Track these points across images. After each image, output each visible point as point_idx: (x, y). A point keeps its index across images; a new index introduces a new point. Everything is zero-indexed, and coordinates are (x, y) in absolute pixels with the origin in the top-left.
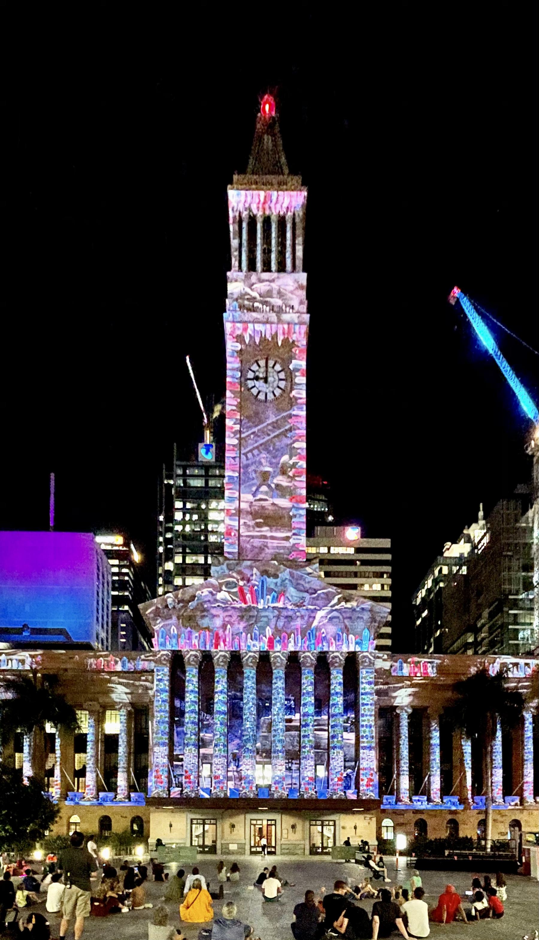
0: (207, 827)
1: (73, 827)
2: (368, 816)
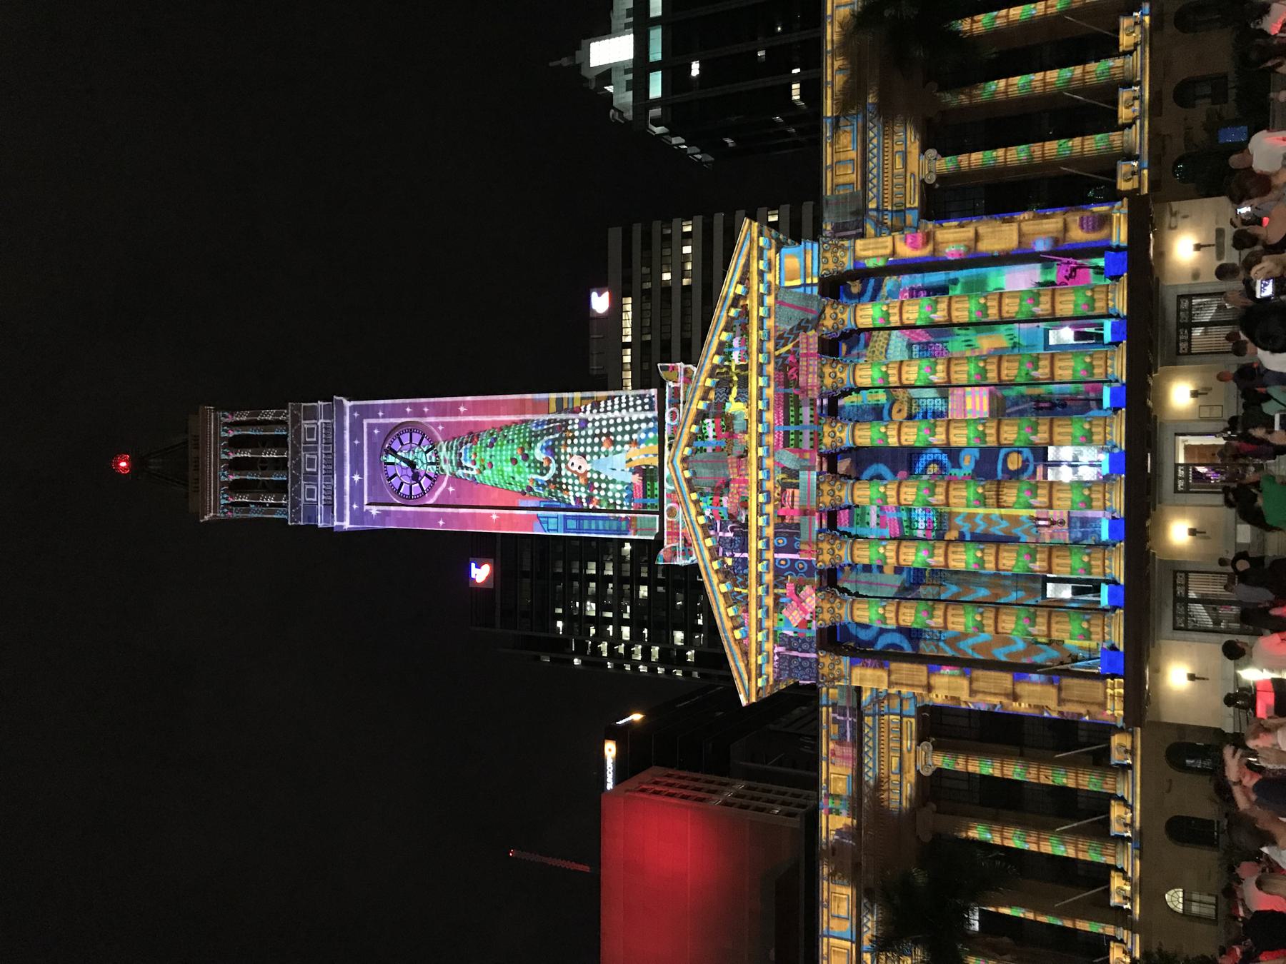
0: (1192, 595)
1: (1195, 909)
2: (1167, 218)
